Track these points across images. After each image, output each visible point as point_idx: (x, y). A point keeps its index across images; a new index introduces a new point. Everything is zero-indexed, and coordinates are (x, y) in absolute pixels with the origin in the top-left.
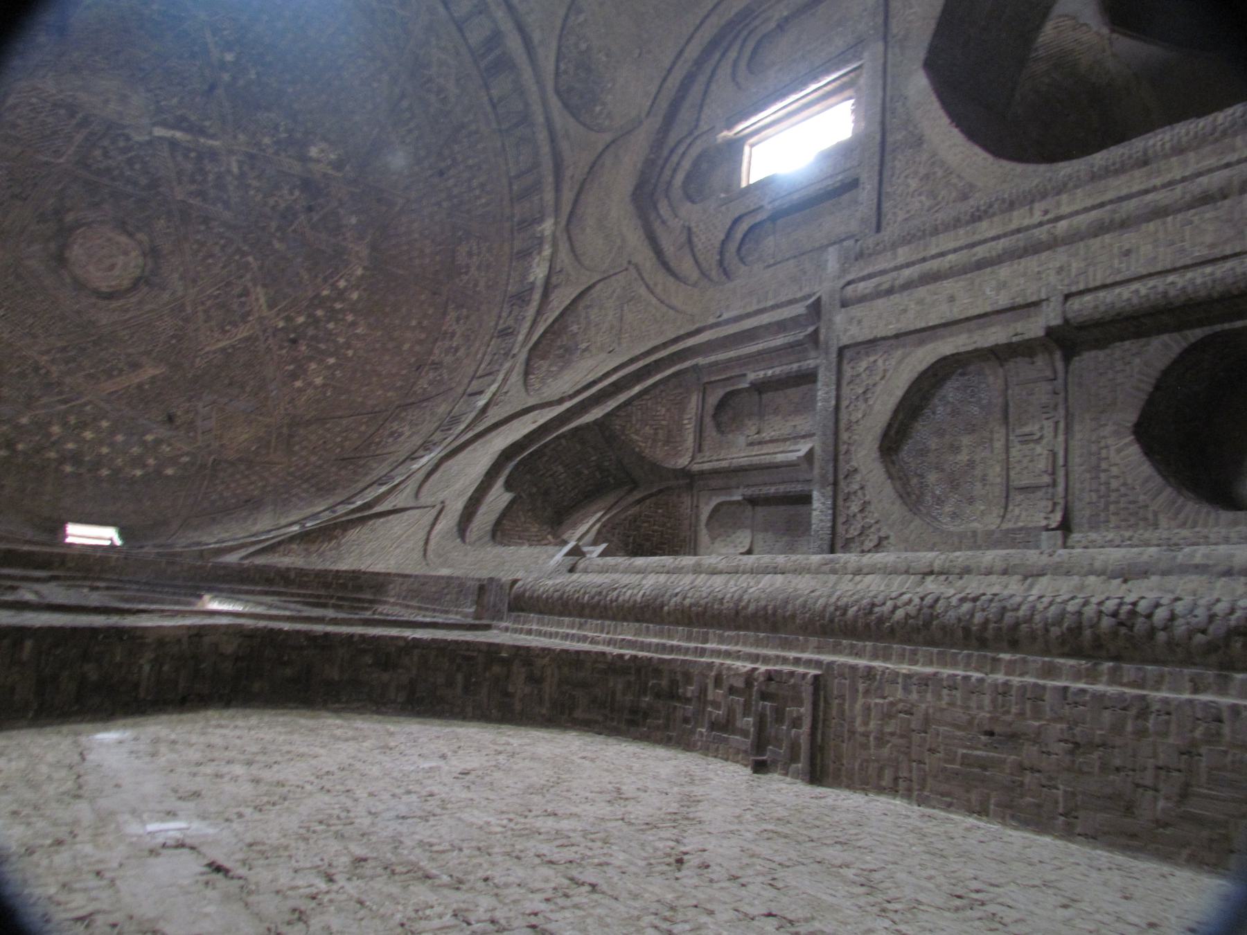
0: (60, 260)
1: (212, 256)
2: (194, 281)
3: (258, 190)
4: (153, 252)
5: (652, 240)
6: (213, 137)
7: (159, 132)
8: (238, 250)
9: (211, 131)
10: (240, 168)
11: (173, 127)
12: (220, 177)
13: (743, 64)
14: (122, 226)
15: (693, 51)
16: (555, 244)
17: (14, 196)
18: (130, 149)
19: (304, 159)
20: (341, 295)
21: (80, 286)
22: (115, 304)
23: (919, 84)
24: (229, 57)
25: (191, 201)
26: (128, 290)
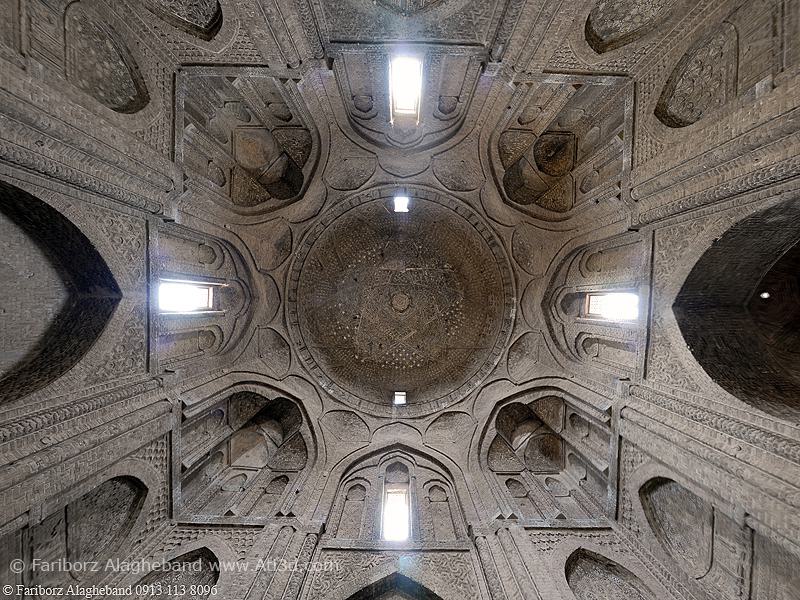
0: (392, 305)
4: (411, 298)
5: (549, 325)
13: (584, 263)
15: (562, 255)
16: (517, 308)
20: (458, 306)
23: (669, 317)
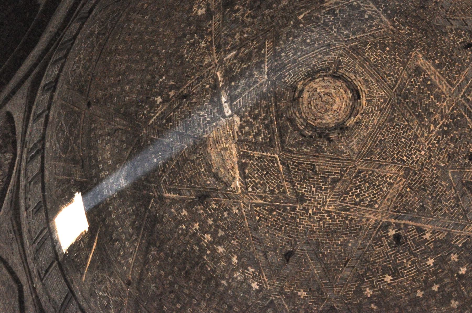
0: (341, 127)
1: (304, 41)
2: (329, 45)
3: (242, 33)
4: (312, 75)
6: (216, 79)
7: (228, 111)
8: (295, 26)
9: (211, 81)
10: (230, 51)
11: (221, 105)
12: (242, 61)
14: (295, 101)
17: (316, 174)
18: (247, 122)
19: (209, 14)
21: (353, 111)
22: (362, 87)
24: (159, 99)
25: (266, 69)
26: (345, 81)
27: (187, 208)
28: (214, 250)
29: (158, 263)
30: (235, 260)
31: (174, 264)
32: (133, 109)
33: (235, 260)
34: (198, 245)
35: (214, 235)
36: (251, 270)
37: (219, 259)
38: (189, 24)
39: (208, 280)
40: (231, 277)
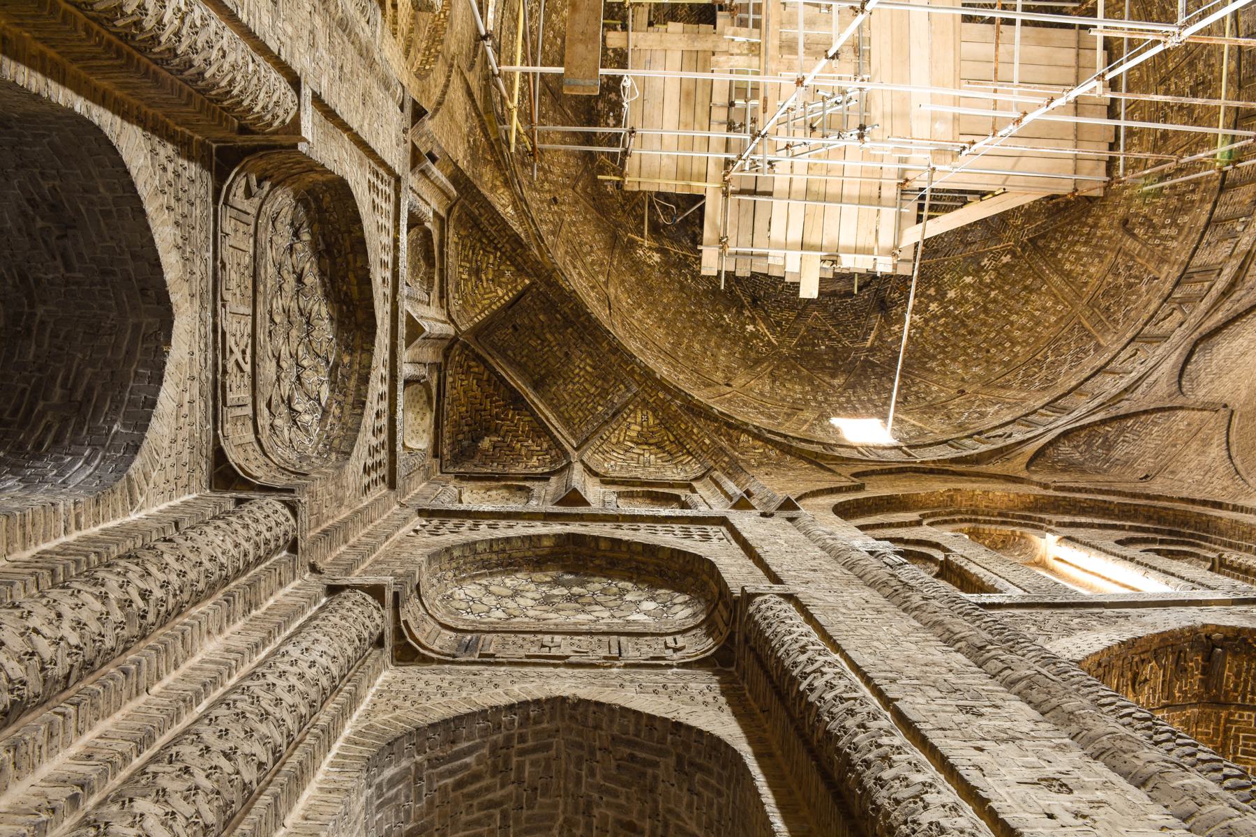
24: (750, 328)
27: (891, 325)
28: (951, 301)
29: (948, 361)
30: (968, 280)
31: (955, 346)
32: (753, 354)
33: (968, 280)
34: (939, 318)
35: (932, 299)
36: (985, 262)
37: (963, 297)
38: (668, 274)
39: (986, 310)
40: (988, 286)
